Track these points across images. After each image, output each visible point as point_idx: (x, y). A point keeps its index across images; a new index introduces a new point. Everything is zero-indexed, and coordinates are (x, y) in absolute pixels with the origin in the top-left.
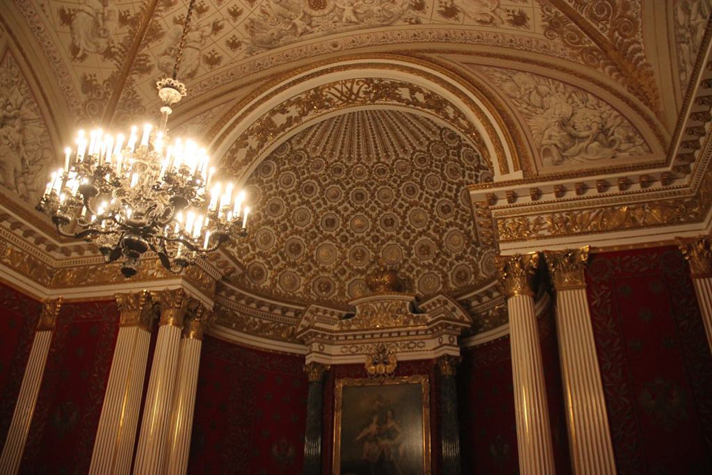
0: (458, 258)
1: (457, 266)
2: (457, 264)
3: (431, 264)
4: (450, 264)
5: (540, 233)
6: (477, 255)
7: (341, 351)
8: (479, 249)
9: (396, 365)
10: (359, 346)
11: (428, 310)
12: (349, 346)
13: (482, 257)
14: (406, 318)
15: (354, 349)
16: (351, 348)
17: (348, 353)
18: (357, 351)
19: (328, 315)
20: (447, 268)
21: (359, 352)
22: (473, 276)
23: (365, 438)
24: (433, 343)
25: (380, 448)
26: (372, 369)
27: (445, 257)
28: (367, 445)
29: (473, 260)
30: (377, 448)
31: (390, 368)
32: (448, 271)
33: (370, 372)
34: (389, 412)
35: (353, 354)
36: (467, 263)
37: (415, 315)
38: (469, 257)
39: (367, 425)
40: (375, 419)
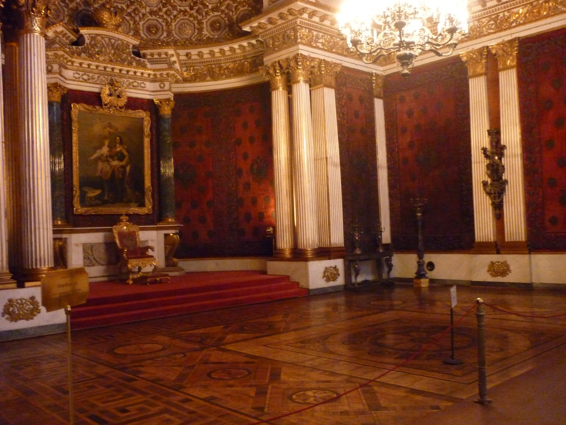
0: (151, 13)
1: (149, 19)
2: (150, 17)
3: (123, 8)
4: (144, 15)
5: (318, 44)
6: (172, 17)
7: (74, 77)
8: (175, 13)
9: (126, 100)
10: (91, 75)
11: (149, 57)
12: (81, 73)
13: (177, 20)
14: (129, 58)
15: (85, 77)
16: (83, 75)
17: (81, 79)
18: (89, 79)
19: (64, 39)
20: (140, 18)
21: (91, 81)
22: (165, 34)
23: (99, 158)
24: (156, 86)
25: (111, 167)
26: (106, 99)
27: (138, 6)
28: (100, 165)
29: (166, 19)
30: (109, 167)
31: (122, 102)
32: (140, 21)
33: (104, 100)
34: (118, 138)
35: (85, 81)
36: (160, 20)
37: (138, 58)
38: (163, 16)
39: (100, 147)
40: (107, 143)
